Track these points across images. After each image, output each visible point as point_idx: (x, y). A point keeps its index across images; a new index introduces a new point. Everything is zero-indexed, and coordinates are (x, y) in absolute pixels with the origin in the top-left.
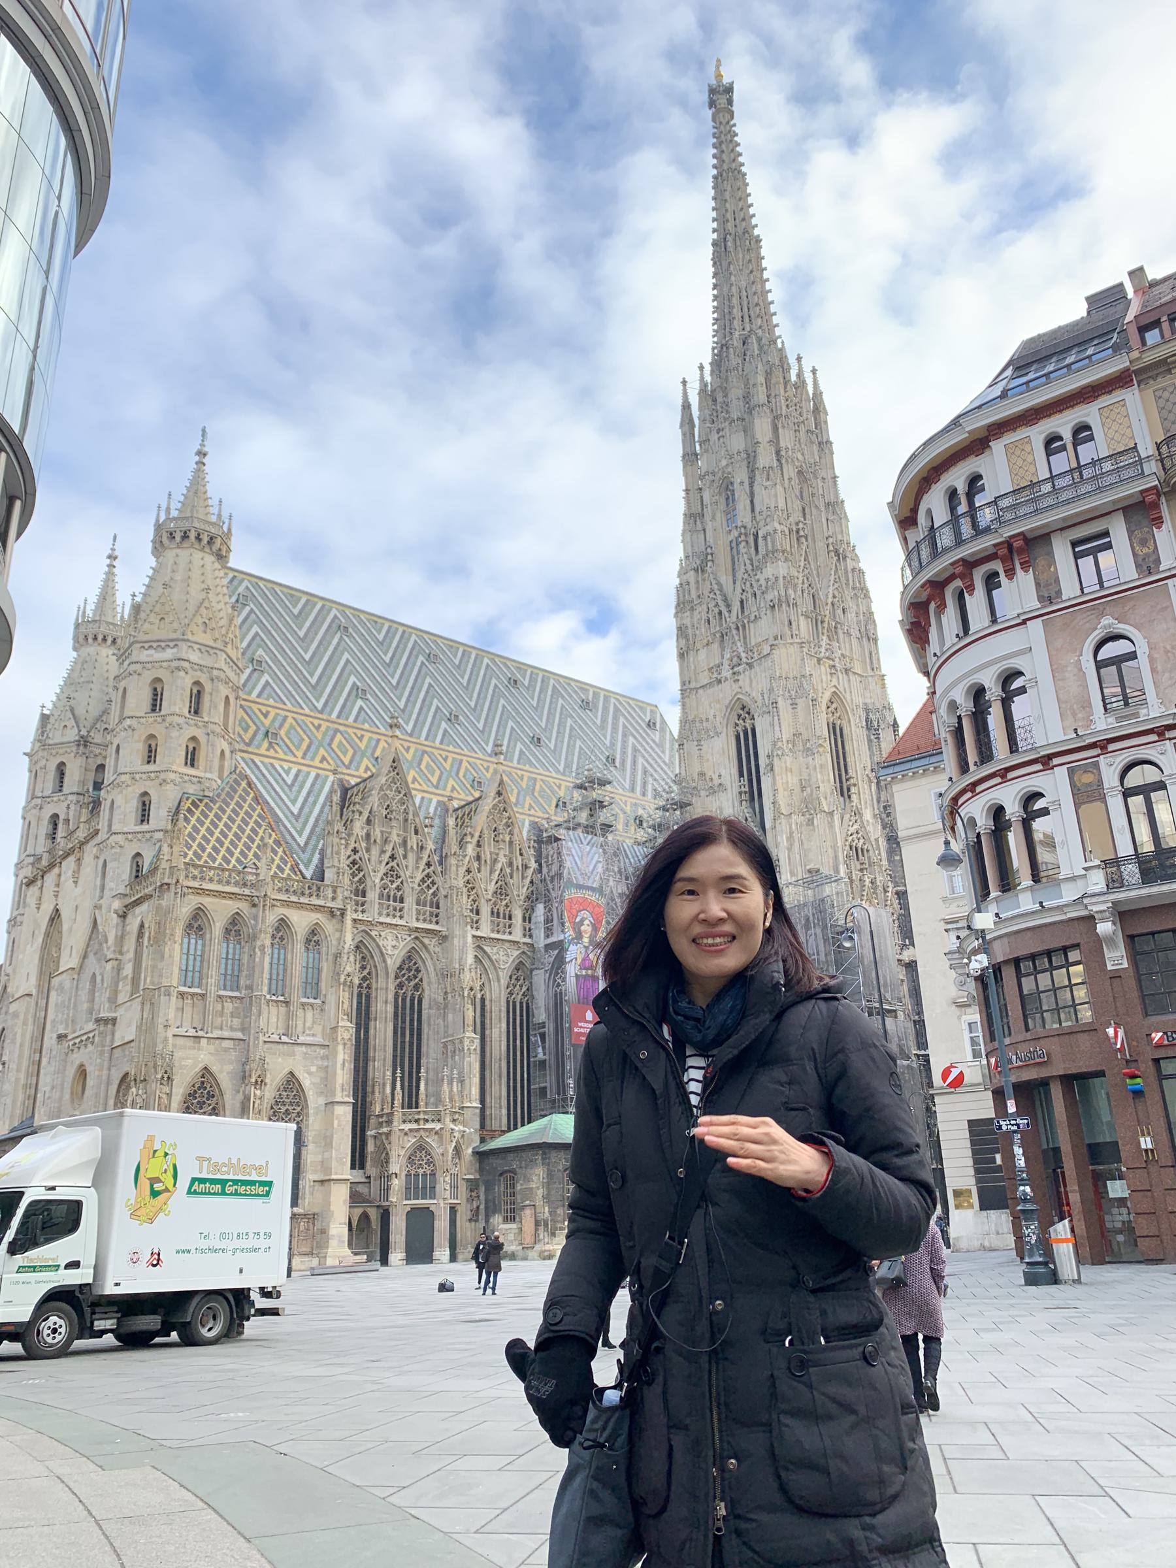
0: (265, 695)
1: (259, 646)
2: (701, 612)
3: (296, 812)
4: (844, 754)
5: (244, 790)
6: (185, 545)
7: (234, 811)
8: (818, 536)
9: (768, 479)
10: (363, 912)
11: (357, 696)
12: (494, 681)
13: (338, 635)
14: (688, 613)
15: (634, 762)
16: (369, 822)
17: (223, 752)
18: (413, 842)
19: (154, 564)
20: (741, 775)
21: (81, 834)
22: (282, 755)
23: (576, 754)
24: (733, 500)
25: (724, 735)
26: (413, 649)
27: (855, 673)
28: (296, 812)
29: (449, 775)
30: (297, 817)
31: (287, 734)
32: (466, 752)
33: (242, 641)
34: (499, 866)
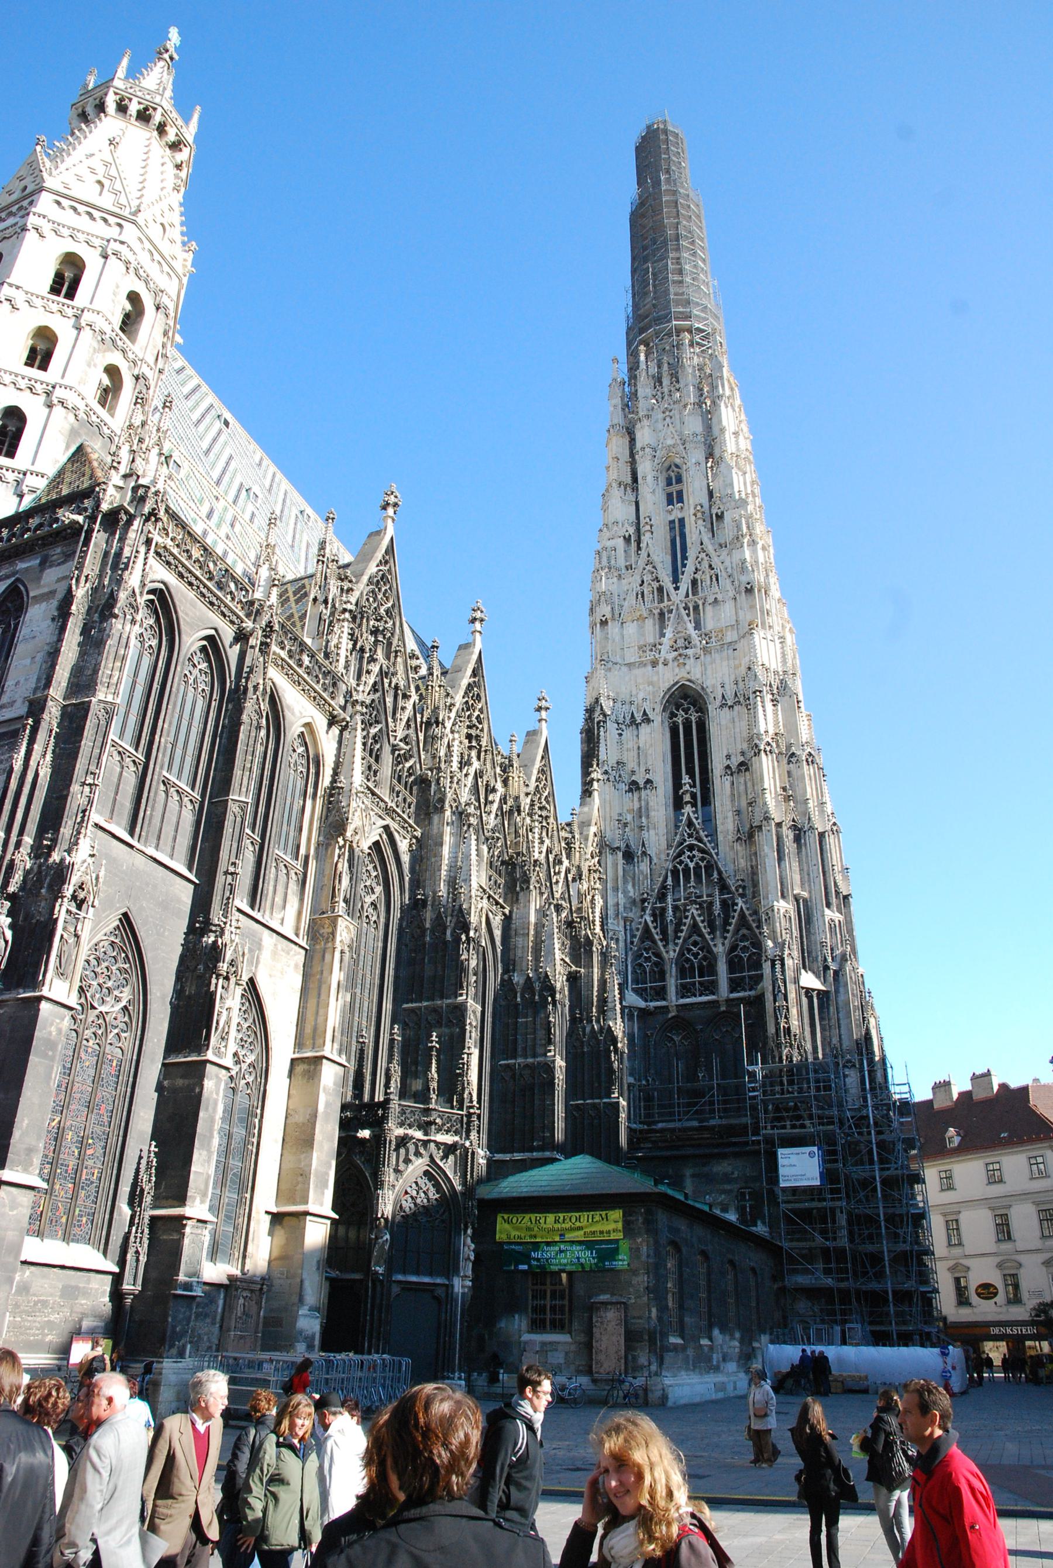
14: (615, 579)
24: (679, 480)
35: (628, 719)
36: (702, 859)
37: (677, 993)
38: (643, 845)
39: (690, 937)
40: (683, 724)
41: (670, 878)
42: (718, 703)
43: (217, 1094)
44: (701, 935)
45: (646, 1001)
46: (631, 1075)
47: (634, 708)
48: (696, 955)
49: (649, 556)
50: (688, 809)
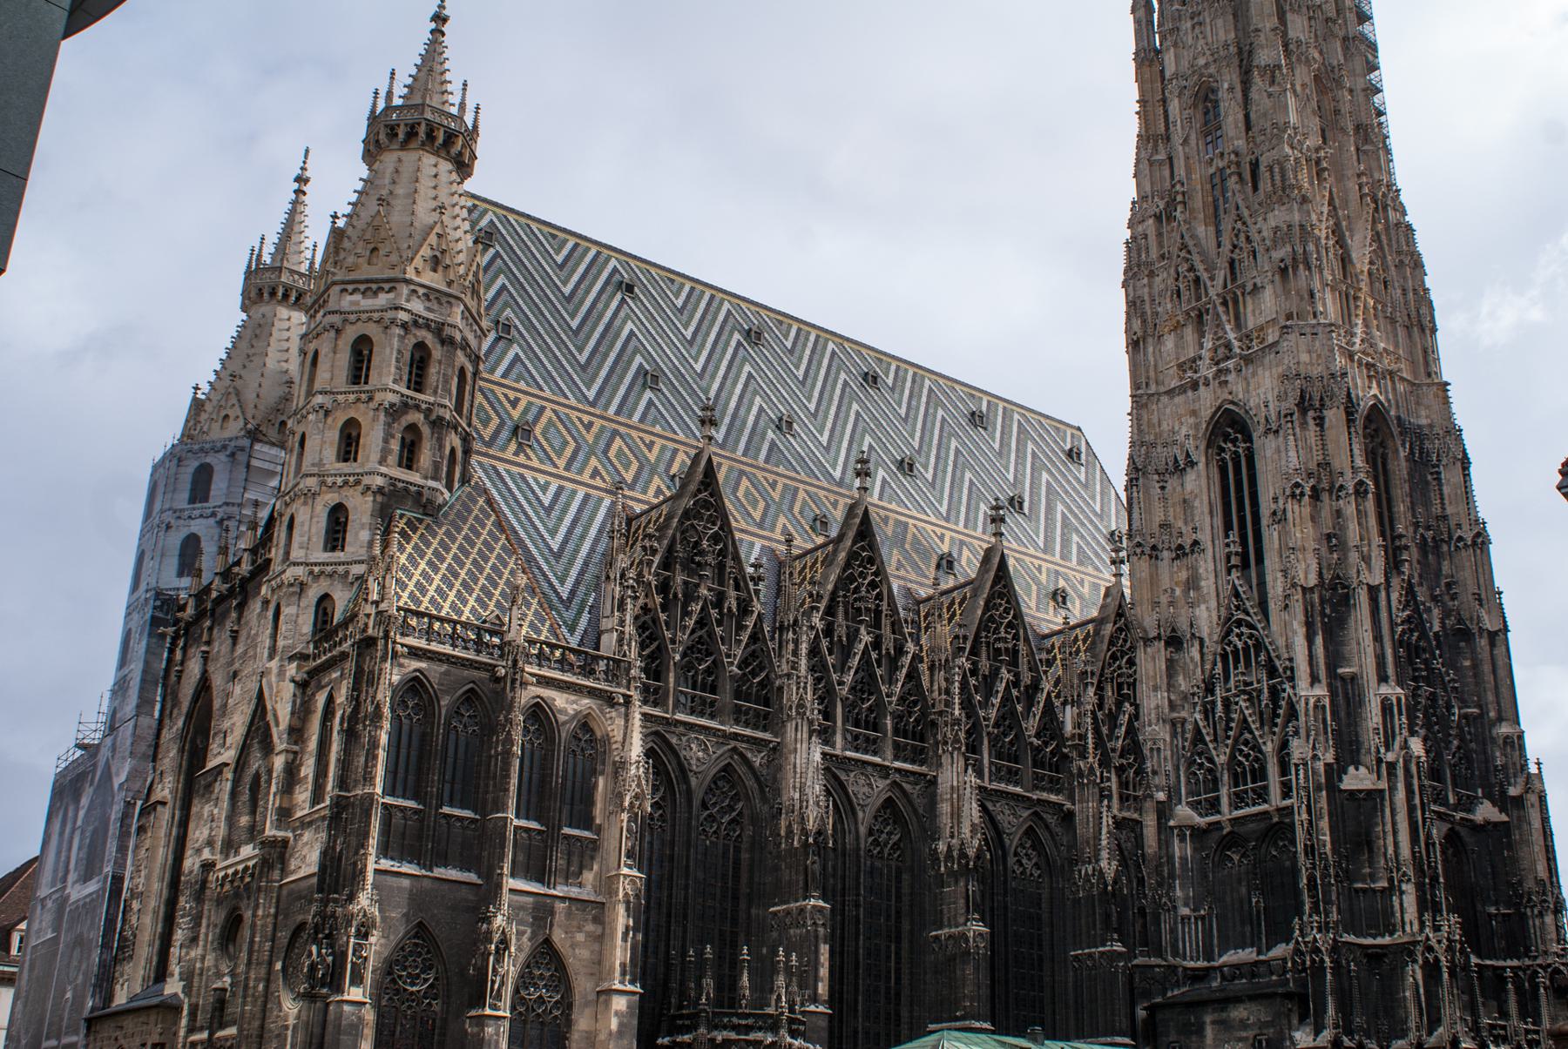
0: (513, 375)
1: (506, 305)
2: (1163, 280)
3: (555, 548)
4: (1389, 500)
5: (482, 510)
6: (412, 146)
7: (466, 538)
8: (1349, 173)
9: (1272, 83)
10: (655, 704)
11: (644, 386)
12: (843, 376)
13: (619, 296)
14: (1145, 281)
15: (1050, 509)
16: (666, 564)
17: (453, 450)
18: (732, 603)
19: (365, 173)
20: (1228, 527)
21: (245, 568)
22: (535, 463)
23: (965, 491)
24: (1217, 115)
25: (1201, 466)
26: (725, 321)
27: (1402, 379)
28: (555, 548)
29: (779, 511)
30: (558, 556)
31: (544, 433)
32: (803, 476)
33: (486, 291)
34: (862, 646)
35: (1171, 464)
36: (1251, 636)
37: (1230, 805)
38: (1192, 625)
39: (1242, 734)
40: (1232, 459)
41: (1219, 665)
42: (1261, 429)
43: (497, 1034)
44: (1251, 732)
45: (1201, 815)
46: (1186, 905)
47: (1178, 453)
48: (1247, 756)
49: (1182, 237)
50: (1235, 574)
